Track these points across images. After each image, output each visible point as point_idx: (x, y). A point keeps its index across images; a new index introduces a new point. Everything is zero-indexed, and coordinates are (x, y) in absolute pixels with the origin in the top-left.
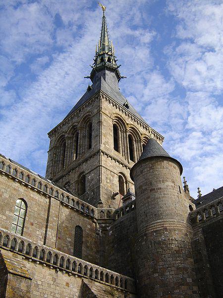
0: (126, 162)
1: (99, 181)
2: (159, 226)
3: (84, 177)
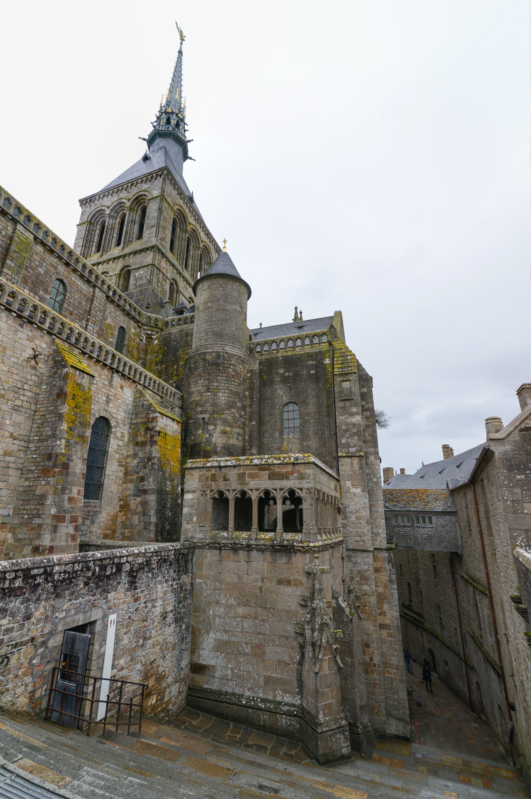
0: (181, 270)
2: (220, 348)
3: (129, 272)
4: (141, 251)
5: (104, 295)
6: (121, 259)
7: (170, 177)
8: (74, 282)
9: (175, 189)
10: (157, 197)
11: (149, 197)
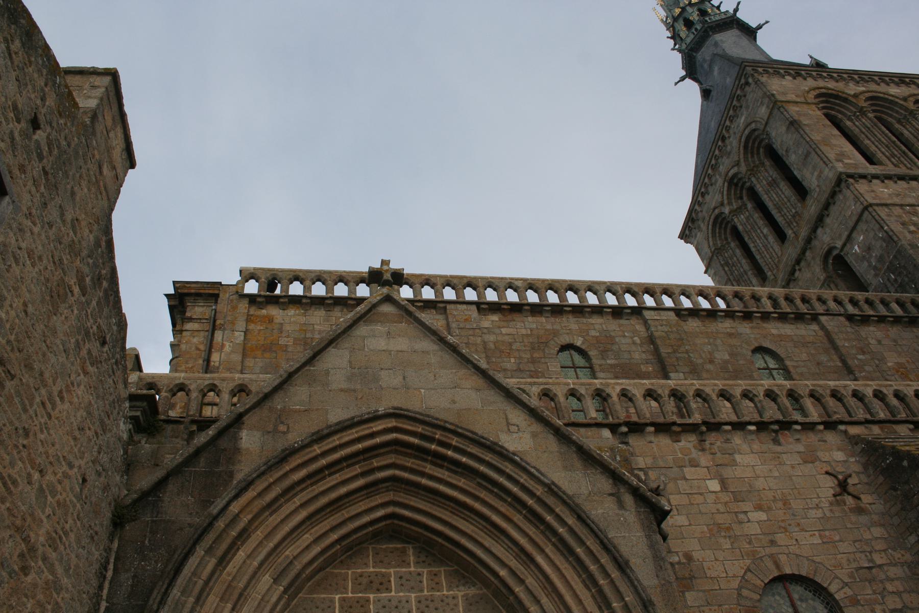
1: (890, 239)
4: (827, 206)
5: (842, 319)
6: (808, 253)
7: (760, 70)
8: (779, 336)
9: (783, 77)
10: (771, 113)
11: (762, 127)
